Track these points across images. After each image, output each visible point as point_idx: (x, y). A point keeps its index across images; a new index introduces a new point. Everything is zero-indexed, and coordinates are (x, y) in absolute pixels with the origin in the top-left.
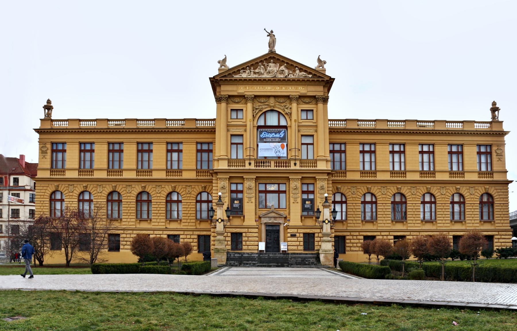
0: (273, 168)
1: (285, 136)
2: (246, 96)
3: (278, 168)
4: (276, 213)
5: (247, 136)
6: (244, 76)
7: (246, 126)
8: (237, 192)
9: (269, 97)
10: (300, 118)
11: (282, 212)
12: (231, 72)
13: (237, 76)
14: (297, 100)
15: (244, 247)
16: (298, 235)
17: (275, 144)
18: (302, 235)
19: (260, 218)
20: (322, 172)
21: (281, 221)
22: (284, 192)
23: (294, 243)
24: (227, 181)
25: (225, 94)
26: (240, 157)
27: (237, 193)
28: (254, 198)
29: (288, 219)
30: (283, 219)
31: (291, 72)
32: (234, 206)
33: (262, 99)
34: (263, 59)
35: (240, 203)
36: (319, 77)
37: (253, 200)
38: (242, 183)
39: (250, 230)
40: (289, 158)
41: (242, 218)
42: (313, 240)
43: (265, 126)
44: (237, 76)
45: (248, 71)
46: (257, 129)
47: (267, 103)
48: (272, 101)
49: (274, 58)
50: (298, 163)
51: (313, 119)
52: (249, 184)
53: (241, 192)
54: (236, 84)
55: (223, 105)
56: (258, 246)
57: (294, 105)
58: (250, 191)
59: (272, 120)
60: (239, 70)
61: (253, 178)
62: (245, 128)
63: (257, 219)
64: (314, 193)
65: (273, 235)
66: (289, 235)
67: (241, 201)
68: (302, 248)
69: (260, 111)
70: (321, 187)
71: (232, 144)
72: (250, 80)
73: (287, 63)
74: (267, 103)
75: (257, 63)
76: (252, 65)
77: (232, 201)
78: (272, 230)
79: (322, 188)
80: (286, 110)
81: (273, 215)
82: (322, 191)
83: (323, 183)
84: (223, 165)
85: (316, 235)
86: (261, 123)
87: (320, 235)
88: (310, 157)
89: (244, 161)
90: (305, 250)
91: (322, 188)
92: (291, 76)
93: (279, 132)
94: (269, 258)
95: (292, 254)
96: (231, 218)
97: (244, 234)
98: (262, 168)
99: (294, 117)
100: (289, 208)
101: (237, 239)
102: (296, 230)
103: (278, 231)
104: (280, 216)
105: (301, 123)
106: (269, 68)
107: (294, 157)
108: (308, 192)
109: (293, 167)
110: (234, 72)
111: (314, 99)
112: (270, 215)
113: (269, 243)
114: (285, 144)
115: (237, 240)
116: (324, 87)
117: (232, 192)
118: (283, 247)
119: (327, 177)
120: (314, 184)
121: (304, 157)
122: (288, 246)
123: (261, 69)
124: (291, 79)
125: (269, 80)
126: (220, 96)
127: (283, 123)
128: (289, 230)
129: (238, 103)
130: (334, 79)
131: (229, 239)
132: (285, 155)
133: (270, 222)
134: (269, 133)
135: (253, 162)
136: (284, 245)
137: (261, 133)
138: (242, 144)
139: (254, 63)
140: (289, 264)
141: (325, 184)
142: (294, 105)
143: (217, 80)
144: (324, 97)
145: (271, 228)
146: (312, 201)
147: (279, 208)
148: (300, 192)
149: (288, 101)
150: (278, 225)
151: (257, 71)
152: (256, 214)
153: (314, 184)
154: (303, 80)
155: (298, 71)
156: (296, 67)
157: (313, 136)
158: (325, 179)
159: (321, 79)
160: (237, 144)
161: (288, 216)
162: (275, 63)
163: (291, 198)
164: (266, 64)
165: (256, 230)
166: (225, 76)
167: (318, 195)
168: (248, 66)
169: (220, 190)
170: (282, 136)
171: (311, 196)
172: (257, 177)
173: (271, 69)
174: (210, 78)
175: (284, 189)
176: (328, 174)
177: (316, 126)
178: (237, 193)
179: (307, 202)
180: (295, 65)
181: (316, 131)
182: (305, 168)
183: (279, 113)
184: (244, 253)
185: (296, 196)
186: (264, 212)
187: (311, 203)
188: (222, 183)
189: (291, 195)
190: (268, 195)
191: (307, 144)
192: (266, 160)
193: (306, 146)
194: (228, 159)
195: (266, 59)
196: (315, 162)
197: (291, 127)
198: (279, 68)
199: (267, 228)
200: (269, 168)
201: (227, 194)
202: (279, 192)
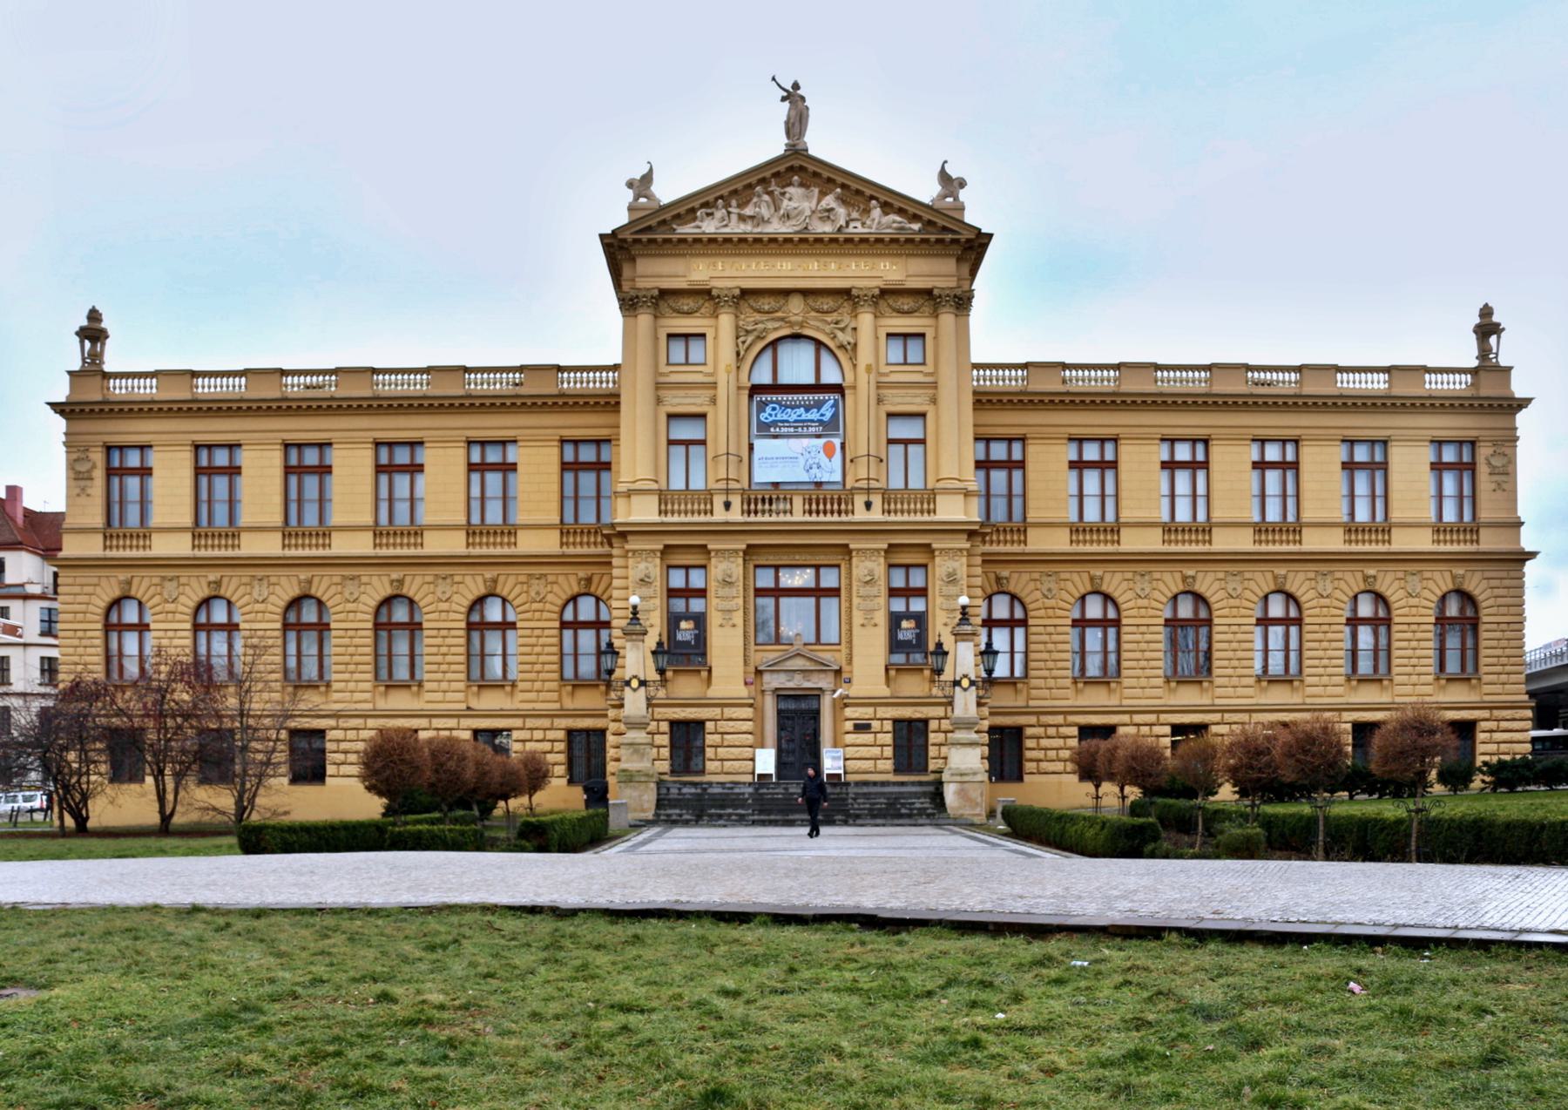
0: (798, 516)
1: (835, 416)
3: (814, 518)
5: (719, 418)
6: (709, 227)
7: (714, 385)
8: (688, 593)
9: (786, 293)
10: (882, 361)
11: (826, 656)
12: (668, 216)
13: (686, 230)
14: (876, 304)
18: (888, 726)
19: (759, 673)
21: (824, 682)
22: (834, 592)
23: (864, 752)
24: (658, 561)
25: (649, 285)
26: (697, 483)
27: (687, 598)
28: (741, 613)
30: (831, 677)
31: (855, 215)
32: (679, 637)
34: (768, 174)
36: (945, 229)
37: (738, 618)
38: (704, 567)
39: (728, 712)
40: (848, 486)
41: (704, 674)
42: (921, 741)
44: (686, 230)
46: (751, 396)
47: (779, 314)
49: (802, 169)
50: (877, 500)
51: (924, 364)
52: (726, 568)
53: (702, 593)
54: (684, 255)
55: (644, 319)
56: (753, 760)
57: (866, 320)
58: (726, 591)
59: (797, 366)
60: (693, 211)
61: (736, 551)
62: (710, 392)
63: (751, 677)
64: (926, 595)
66: (849, 726)
67: (700, 620)
68: (888, 765)
69: (759, 338)
70: (949, 575)
71: (671, 443)
72: (727, 241)
73: (843, 186)
74: (779, 314)
75: (750, 186)
76: (735, 192)
77: (673, 621)
78: (795, 711)
79: (952, 579)
80: (839, 334)
81: (799, 663)
82: (953, 590)
83: (956, 565)
84: (644, 511)
85: (933, 725)
86: (763, 376)
87: (945, 724)
88: (916, 483)
89: (709, 494)
90: (897, 771)
95: (857, 784)
96: (669, 674)
97: (709, 726)
98: (766, 518)
99: (865, 355)
100: (850, 642)
101: (687, 739)
104: (823, 668)
105: (886, 375)
106: (786, 202)
107: (863, 484)
108: (907, 592)
109: (860, 515)
110: (678, 217)
114: (837, 442)
117: (672, 593)
118: (831, 763)
119: (968, 545)
120: (925, 566)
121: (897, 482)
123: (760, 206)
124: (856, 238)
125: (788, 241)
126: (633, 293)
127: (830, 375)
128: (849, 712)
129: (689, 313)
130: (990, 236)
131: (664, 740)
132: (837, 477)
135: (736, 501)
136: (834, 758)
138: (703, 443)
139: (739, 186)
140: (849, 816)
142: (866, 320)
143: (625, 240)
144: (958, 292)
145: (792, 705)
146: (921, 619)
148: (884, 591)
149: (847, 307)
150: (816, 695)
153: (925, 566)
154: (893, 241)
155: (876, 213)
158: (961, 550)
160: (687, 443)
161: (846, 668)
163: (855, 613)
164: (778, 191)
165: (747, 712)
166: (649, 229)
167: (939, 600)
168: (721, 197)
169: (637, 587)
171: (917, 605)
172: (749, 546)
173: (793, 204)
175: (835, 585)
176: (971, 534)
177: (934, 385)
178: (687, 598)
179: (905, 624)
180: (868, 192)
181: (934, 401)
182: (899, 518)
183: (819, 344)
184: (710, 784)
185: (869, 604)
187: (918, 626)
188: (642, 566)
189: (856, 601)
190: (784, 601)
191: (906, 442)
192: (776, 493)
194: (660, 492)
195: (777, 175)
197: (854, 388)
198: (819, 201)
199: (783, 706)
201: (657, 602)
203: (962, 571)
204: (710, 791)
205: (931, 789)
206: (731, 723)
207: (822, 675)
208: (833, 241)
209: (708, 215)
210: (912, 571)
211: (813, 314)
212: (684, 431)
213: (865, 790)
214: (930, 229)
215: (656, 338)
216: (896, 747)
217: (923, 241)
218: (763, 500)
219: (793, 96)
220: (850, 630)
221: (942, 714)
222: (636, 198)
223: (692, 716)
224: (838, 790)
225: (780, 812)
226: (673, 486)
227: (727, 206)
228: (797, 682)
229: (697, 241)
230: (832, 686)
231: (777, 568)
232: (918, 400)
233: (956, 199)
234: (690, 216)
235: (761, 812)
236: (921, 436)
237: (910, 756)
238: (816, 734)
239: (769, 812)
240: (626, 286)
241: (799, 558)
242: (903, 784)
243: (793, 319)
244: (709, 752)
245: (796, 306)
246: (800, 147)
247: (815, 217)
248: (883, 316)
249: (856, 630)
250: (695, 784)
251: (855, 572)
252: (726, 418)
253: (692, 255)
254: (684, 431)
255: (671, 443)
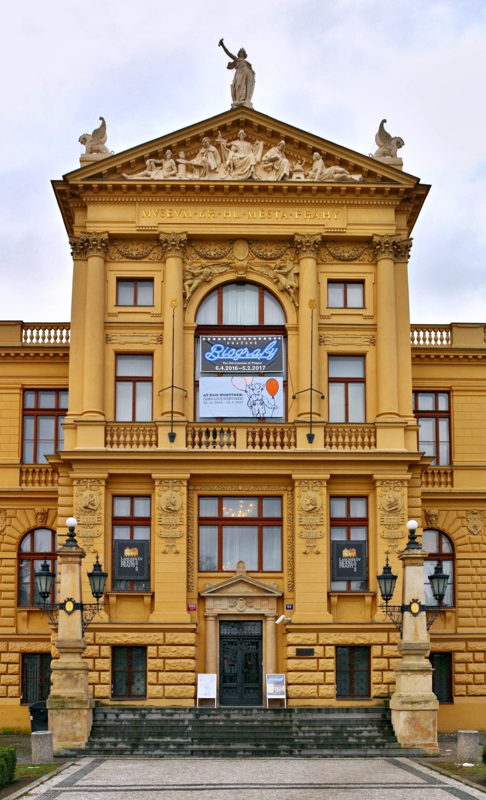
0: (241, 447)
1: (278, 356)
2: (162, 237)
3: (257, 449)
4: (252, 586)
5: (165, 355)
6: (158, 175)
7: (161, 325)
10: (324, 305)
11: (269, 583)
13: (138, 177)
14: (317, 251)
15: (152, 690)
16: (318, 650)
17: (249, 379)
18: (331, 651)
19: (202, 599)
20: (390, 461)
21: (266, 608)
22: (277, 522)
23: (306, 677)
24: (102, 489)
25: (99, 230)
26: (143, 415)
27: (132, 527)
28: (184, 540)
29: (287, 602)
30: (273, 604)
31: (298, 167)
32: (123, 564)
33: (213, 247)
34: (214, 127)
35: (140, 555)
36: (384, 180)
37: (181, 545)
38: (149, 496)
39: (171, 637)
40: (291, 420)
41: (147, 600)
42: (362, 667)
43: (221, 329)
44: (138, 177)
45: (168, 163)
46: (196, 337)
47: (225, 260)
48: (241, 254)
49: (247, 124)
50: (319, 433)
51: (364, 308)
52: (170, 494)
53: (146, 522)
54: (133, 203)
55: (95, 262)
57: (308, 265)
58: (170, 519)
59: (241, 309)
60: (142, 160)
61: (180, 480)
62: (159, 332)
63: (194, 603)
64: (367, 526)
65: (242, 657)
66: (291, 651)
67: (144, 548)
68: (331, 690)
69: (206, 282)
70: (391, 505)
71: (119, 379)
72: (175, 188)
73: (288, 140)
74: (225, 260)
75: (197, 139)
76: (183, 144)
77: (118, 548)
78: (238, 637)
79: (393, 508)
80: (282, 279)
81: (242, 590)
82: (394, 519)
83: (397, 495)
84: (90, 441)
85: (375, 651)
86: (209, 317)
87: (389, 650)
88: (356, 416)
89: (154, 425)
90: (339, 696)
91: (393, 508)
92: (299, 178)
93: (262, 346)
94: (230, 724)
95: (301, 710)
96: (113, 599)
97: (151, 651)
98: (211, 449)
100: (292, 569)
101: (129, 662)
102: (313, 636)
103: (258, 641)
104: (265, 595)
105: (328, 317)
106: (231, 153)
107: (306, 418)
108: (348, 523)
109: (303, 446)
110: (127, 166)
111: (368, 245)
112: (232, 591)
113: (232, 679)
114: (280, 380)
115: (130, 666)
116: (398, 211)
117: (117, 522)
118: (273, 688)
119: (409, 476)
120: (366, 497)
121: (337, 416)
122: (288, 684)
123: (208, 157)
124: (300, 186)
125: (233, 189)
126: (84, 237)
127: (273, 318)
128: (291, 638)
129: (138, 258)
130: (429, 187)
131: (106, 664)
132: (280, 413)
133: (233, 611)
134: (231, 347)
135: (181, 432)
136: (277, 684)
137: (208, 346)
138: (149, 380)
139: (187, 137)
140: (294, 745)
141: (400, 495)
142: (308, 265)
143: (75, 187)
144: (397, 239)
145: (234, 631)
146: (362, 549)
147: (260, 569)
148: (326, 521)
149: (290, 254)
150: (259, 620)
151: (197, 161)
152: (189, 589)
153: (366, 497)
154: (335, 190)
155: (319, 164)
156: (314, 150)
157: (363, 356)
158: (402, 481)
159: (388, 187)
160: (135, 380)
161: (288, 595)
162: (252, 142)
163: (298, 540)
164: (224, 142)
165: (190, 637)
166: (100, 176)
167: (380, 529)
168: (170, 147)
169: (82, 509)
170: (271, 355)
171: (358, 535)
172: (192, 476)
173: (238, 155)
174: (53, 182)
175: (277, 515)
176: (412, 466)
177: (374, 327)
178: (132, 527)
179: (346, 553)
180: (311, 145)
181: (373, 342)
182: (341, 449)
183: (263, 289)
184: (150, 710)
185: (312, 533)
186: (215, 583)
187: (359, 555)
188: (87, 493)
189: (298, 529)
190: (227, 531)
191: (347, 381)
192: (221, 426)
193: (342, 386)
194: (106, 424)
195: (223, 129)
196: (370, 429)
197: (297, 329)
198: (263, 155)
199: (225, 631)
200: (232, 449)
201: (101, 529)
202: (259, 522)
203: (403, 502)
204: (149, 717)
205: (378, 716)
206: (174, 648)
207: (265, 602)
208: (277, 189)
209: (157, 165)
210: (353, 502)
211: (257, 260)
212: (129, 368)
213: (310, 717)
214: (369, 180)
215: (106, 281)
216: (338, 671)
217: (365, 191)
218: (208, 432)
219: (239, 62)
220: (293, 558)
221: (385, 640)
222: (91, 151)
223: (134, 641)
224: (281, 717)
225: (221, 740)
226: (120, 418)
227: (175, 156)
228: (240, 608)
229: (146, 188)
230: (274, 612)
231: (220, 498)
232: (358, 341)
233: (394, 155)
234: (141, 166)
235: (201, 741)
236: (360, 375)
237: (352, 682)
238: (258, 658)
239: (209, 741)
240: (77, 232)
241: (242, 490)
242: (348, 710)
243: (238, 264)
244: (151, 677)
245: (241, 254)
246: (247, 105)
247: (260, 168)
248: (324, 263)
249: (299, 558)
250: (133, 710)
251: (297, 501)
252: (172, 355)
253: (141, 203)
254: (129, 368)
255: (119, 379)
